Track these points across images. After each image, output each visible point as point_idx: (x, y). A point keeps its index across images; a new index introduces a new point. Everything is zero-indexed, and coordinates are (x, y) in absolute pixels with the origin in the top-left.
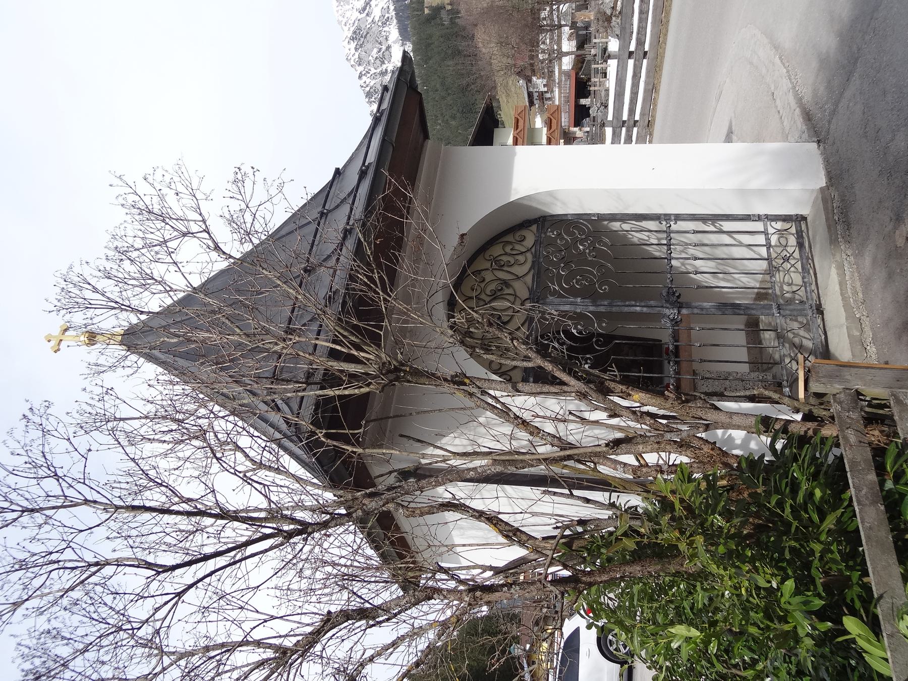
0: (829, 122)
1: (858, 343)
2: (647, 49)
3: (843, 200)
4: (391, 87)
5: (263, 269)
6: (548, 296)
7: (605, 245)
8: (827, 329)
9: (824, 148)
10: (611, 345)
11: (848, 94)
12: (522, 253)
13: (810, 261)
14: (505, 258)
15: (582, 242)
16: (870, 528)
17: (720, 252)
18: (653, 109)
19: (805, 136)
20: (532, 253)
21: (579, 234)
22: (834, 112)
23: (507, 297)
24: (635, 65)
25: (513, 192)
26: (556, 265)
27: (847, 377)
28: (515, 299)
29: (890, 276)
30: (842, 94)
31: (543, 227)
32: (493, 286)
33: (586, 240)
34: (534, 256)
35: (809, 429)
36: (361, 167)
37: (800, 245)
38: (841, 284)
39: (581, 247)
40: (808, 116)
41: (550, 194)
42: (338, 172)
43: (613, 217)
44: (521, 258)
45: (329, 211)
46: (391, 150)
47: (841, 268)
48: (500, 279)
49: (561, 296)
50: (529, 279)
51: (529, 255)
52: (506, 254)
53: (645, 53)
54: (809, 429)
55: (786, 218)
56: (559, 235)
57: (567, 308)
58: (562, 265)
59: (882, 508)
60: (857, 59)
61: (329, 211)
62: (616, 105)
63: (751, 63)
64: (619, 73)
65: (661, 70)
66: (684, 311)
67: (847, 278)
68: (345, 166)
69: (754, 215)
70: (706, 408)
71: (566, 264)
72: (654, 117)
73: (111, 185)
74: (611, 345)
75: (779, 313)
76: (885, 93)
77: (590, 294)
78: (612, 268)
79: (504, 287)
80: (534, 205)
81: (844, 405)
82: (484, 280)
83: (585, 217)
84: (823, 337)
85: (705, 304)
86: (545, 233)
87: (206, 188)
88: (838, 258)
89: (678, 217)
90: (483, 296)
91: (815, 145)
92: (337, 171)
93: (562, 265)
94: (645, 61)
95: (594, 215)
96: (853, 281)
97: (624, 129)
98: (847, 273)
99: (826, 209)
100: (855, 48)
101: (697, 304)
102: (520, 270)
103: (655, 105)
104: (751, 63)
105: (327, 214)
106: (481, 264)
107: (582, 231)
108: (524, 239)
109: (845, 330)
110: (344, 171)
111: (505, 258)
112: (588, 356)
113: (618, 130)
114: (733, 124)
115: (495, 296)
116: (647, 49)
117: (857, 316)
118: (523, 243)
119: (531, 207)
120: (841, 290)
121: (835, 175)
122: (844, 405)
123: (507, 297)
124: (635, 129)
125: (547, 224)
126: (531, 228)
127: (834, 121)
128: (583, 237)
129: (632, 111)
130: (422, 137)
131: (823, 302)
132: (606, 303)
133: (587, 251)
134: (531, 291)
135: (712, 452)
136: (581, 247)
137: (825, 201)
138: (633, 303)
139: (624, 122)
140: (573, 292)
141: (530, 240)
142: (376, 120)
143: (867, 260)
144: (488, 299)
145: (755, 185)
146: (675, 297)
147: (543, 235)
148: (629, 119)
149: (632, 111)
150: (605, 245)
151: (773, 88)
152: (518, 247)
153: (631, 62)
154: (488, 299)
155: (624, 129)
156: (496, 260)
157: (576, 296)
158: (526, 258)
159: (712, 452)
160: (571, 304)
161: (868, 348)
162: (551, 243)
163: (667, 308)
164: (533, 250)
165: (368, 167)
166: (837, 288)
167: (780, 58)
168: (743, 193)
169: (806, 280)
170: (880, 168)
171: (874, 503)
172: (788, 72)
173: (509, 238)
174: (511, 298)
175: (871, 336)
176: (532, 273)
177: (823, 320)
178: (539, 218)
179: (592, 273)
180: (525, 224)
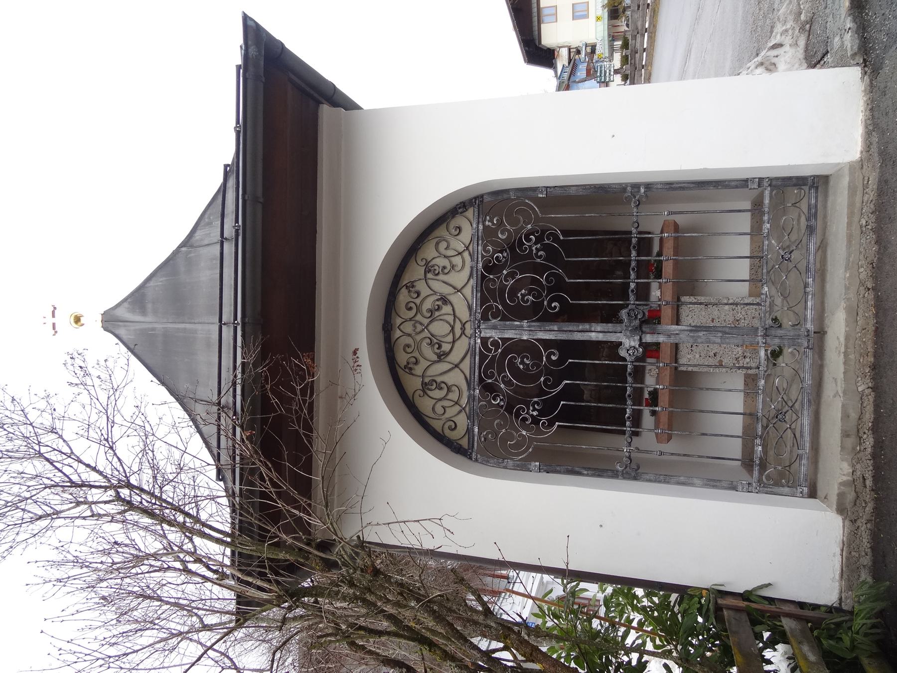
10: (561, 387)
12: (460, 253)
28: (454, 320)
32: (428, 305)
44: (457, 260)
49: (504, 318)
50: (468, 291)
51: (466, 254)
56: (500, 223)
57: (509, 334)
74: (561, 387)
82: (418, 294)
90: (419, 317)
92: (226, 166)
106: (416, 272)
111: (441, 262)
112: (536, 399)
126: (467, 214)
128: (529, 226)
144: (426, 321)
154: (426, 321)
157: (521, 319)
158: (464, 262)
173: (441, 231)
176: (472, 282)
178: (476, 198)
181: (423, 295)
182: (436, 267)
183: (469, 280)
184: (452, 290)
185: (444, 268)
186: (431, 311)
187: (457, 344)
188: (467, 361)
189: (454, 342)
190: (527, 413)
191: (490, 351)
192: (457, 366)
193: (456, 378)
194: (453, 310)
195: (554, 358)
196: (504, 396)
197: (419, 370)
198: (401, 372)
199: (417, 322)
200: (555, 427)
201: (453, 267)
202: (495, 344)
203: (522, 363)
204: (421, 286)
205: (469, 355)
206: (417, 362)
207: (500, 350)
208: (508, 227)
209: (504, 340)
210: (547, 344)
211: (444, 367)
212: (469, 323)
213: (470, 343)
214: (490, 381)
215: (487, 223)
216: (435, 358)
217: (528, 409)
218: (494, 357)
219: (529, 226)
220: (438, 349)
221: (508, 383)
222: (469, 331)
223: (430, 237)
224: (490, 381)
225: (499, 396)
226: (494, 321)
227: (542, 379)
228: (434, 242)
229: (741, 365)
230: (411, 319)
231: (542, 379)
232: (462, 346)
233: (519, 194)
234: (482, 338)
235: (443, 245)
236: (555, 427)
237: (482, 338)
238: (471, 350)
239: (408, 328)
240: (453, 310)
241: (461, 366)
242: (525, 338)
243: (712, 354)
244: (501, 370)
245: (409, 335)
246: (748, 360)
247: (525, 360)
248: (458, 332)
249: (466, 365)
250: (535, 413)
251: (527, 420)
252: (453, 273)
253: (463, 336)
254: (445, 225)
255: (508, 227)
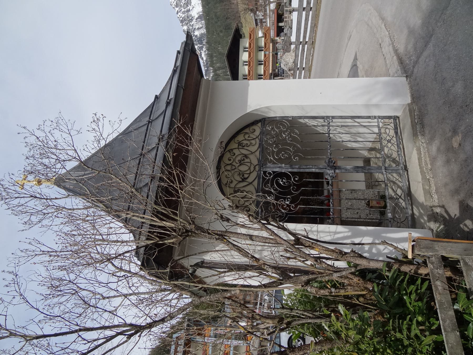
0: (414, 67)
1: (428, 193)
2: (312, 6)
3: (420, 111)
4: (182, 52)
5: (111, 174)
6: (268, 163)
7: (296, 134)
8: (410, 180)
9: (410, 81)
10: (300, 191)
11: (425, 54)
13: (401, 141)
14: (245, 142)
15: (284, 132)
16: (452, 347)
17: (353, 130)
18: (315, 36)
19: (400, 72)
20: (259, 139)
21: (283, 128)
22: (416, 62)
23: (247, 164)
24: (306, 15)
25: (248, 107)
26: (271, 145)
27: (437, 248)
29: (448, 162)
30: (421, 53)
31: (264, 124)
32: (239, 158)
33: (286, 131)
34: (260, 141)
35: (412, 270)
36: (167, 100)
37: (396, 133)
38: (419, 159)
39: (284, 135)
40: (401, 61)
41: (267, 108)
42: (157, 97)
43: (300, 117)
44: (253, 142)
45: (153, 121)
46: (182, 91)
47: (419, 150)
48: (243, 154)
49: (274, 163)
50: (258, 153)
51: (257, 140)
52: (246, 140)
53: (311, 8)
54: (412, 270)
55: (389, 117)
56: (272, 128)
57: (277, 170)
58: (274, 146)
59: (458, 333)
60: (432, 36)
61: (153, 121)
62: (297, 34)
63: (368, 25)
64: (299, 20)
65: (319, 17)
66: (337, 171)
67: (422, 156)
68: (160, 94)
69: (372, 116)
70: (356, 256)
71: (276, 145)
72: (315, 39)
73: (18, 133)
74: (300, 191)
75: (386, 172)
76: (449, 59)
77: (288, 161)
78: (300, 147)
79: (245, 158)
80: (259, 113)
81: (434, 265)
82: (235, 154)
83: (286, 118)
84: (407, 183)
85: (348, 167)
86: (265, 128)
87: (76, 127)
88: (417, 145)
89: (333, 117)
90: (234, 164)
91: (405, 79)
92: (156, 96)
93: (274, 146)
94: (311, 12)
95: (290, 117)
96: (425, 158)
97: (301, 46)
98: (422, 153)
99: (411, 116)
100: (431, 28)
101: (343, 167)
102: (253, 149)
103: (316, 34)
104: (368, 25)
105: (151, 122)
106: (233, 145)
107: (284, 126)
108: (254, 131)
109: (421, 186)
110: (160, 97)
111: (245, 142)
112: (289, 197)
113: (298, 46)
114: (357, 55)
115: (241, 163)
116: (312, 6)
117: (428, 178)
118: (254, 133)
119: (257, 114)
120: (419, 162)
121: (416, 98)
122: (434, 265)
123: (247, 164)
124: (306, 46)
125: (266, 123)
126: (258, 125)
127: (416, 66)
128: (285, 129)
129: (305, 37)
130: (200, 76)
131: (408, 165)
132: (297, 167)
133: (287, 138)
134: (259, 160)
135: (358, 282)
136: (284, 135)
137: (410, 111)
138: (311, 167)
139: (301, 42)
140: (280, 161)
141: (257, 132)
142: (174, 71)
143: (434, 148)
145: (375, 101)
146: (333, 164)
147: (264, 129)
148: (303, 41)
149: (305, 37)
150: (296, 134)
151: (380, 41)
152: (251, 135)
153: (304, 13)
155: (301, 46)
156: (240, 144)
157: (282, 163)
158: (256, 142)
159: (358, 282)
160: (280, 167)
161: (433, 196)
162: (268, 133)
163: (329, 169)
164: (259, 137)
165: (170, 100)
166: (417, 161)
167: (385, 25)
168: (367, 106)
169: (399, 153)
170: (444, 100)
171: (453, 330)
172: (389, 34)
173: (247, 130)
174: (249, 164)
175: (435, 189)
176: (259, 150)
177: (408, 174)
178: (262, 119)
179: (290, 150)
180: (255, 123)
181: (236, 155)
182: (243, 144)
183: (258, 149)
184: (249, 153)
185: (247, 144)
186: (240, 161)
187: (252, 175)
188: (256, 182)
189: (250, 173)
190: (284, 203)
191: (267, 176)
192: (251, 183)
193: (251, 188)
194: (250, 160)
195: (296, 179)
196: (273, 195)
197: (232, 185)
198: (223, 186)
199: (233, 165)
200: (298, 208)
201: (251, 143)
202: (270, 174)
203: (282, 181)
204: (237, 152)
205: (257, 178)
206: (232, 182)
207: (272, 176)
208: (276, 130)
209: (274, 172)
210: (293, 173)
211: (245, 184)
212: (257, 166)
213: (258, 174)
214: (267, 189)
215: (267, 128)
216: (241, 180)
217: (285, 201)
218: (269, 179)
219: (285, 129)
220: (242, 176)
221: (276, 190)
222: (257, 168)
223: (242, 132)
224: (267, 189)
225: (271, 196)
226: (269, 164)
227: (292, 188)
228: (243, 134)
229: (369, 218)
230: (230, 164)
231: (292, 188)
232: (254, 175)
233: (281, 118)
234: (264, 172)
235: (247, 136)
236: (298, 208)
237: (264, 172)
238: (258, 176)
239: (229, 168)
240: (250, 160)
241: (253, 183)
242: (283, 171)
243: (356, 213)
244: (272, 185)
245: (229, 171)
246: (372, 215)
247: (284, 180)
248: (252, 169)
249: (256, 183)
250: (288, 203)
251: (284, 206)
252: (251, 146)
253: (255, 171)
254: (248, 128)
255: (276, 130)
